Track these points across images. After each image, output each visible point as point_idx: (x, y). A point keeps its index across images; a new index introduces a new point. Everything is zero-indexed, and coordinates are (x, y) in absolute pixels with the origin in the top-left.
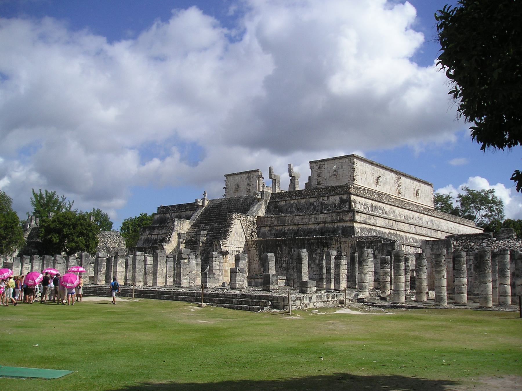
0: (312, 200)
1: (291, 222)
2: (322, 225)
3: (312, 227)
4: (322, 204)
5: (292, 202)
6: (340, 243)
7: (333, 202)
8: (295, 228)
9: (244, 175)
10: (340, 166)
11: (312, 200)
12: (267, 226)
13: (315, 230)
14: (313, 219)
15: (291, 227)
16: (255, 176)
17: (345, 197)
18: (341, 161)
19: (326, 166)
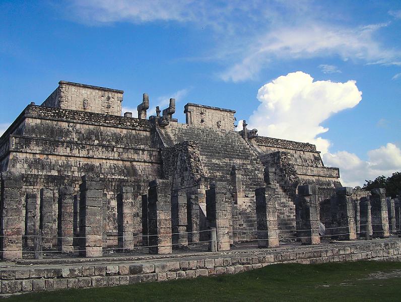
9: (97, 91)
17: (316, 155)
18: (222, 113)
19: (207, 114)
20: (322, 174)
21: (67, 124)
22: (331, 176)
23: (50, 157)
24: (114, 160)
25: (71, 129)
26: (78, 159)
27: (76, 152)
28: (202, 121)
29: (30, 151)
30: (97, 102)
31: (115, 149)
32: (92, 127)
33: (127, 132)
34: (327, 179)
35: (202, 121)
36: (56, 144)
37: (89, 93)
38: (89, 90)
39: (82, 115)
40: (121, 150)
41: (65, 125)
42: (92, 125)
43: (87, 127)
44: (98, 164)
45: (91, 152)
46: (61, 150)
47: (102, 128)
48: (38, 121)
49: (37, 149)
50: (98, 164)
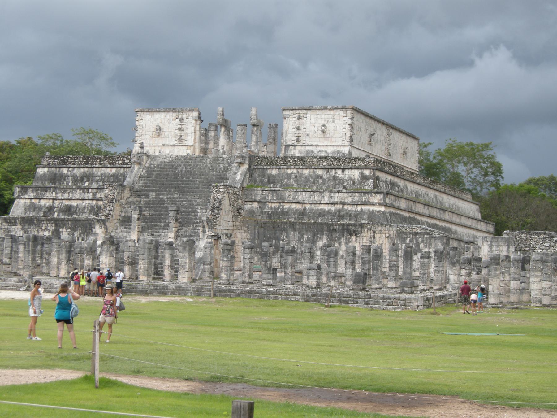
0: (319, 172)
1: (294, 199)
2: (339, 207)
3: (326, 208)
4: (335, 178)
5: (289, 171)
6: (374, 232)
7: (350, 177)
8: (299, 207)
10: (331, 120)
11: (319, 172)
12: (255, 201)
13: (329, 212)
14: (326, 199)
15: (293, 206)
16: (190, 118)
17: (367, 172)
18: (332, 113)
19: (308, 117)
20: (349, 199)
21: (67, 169)
22: (365, 204)
23: (42, 201)
24: (90, 200)
25: (69, 173)
26: (61, 201)
27: (59, 196)
28: (298, 129)
29: (27, 197)
30: (170, 125)
31: (90, 190)
32: (86, 169)
33: (116, 171)
34: (359, 208)
35: (298, 129)
36: (45, 190)
37: (163, 117)
38: (163, 113)
39: (81, 159)
40: (95, 191)
41: (65, 171)
42: (87, 167)
43: (82, 170)
44: (75, 204)
45: (71, 194)
46: (48, 195)
47: (95, 169)
48: (46, 169)
49: (32, 195)
50: (75, 204)
